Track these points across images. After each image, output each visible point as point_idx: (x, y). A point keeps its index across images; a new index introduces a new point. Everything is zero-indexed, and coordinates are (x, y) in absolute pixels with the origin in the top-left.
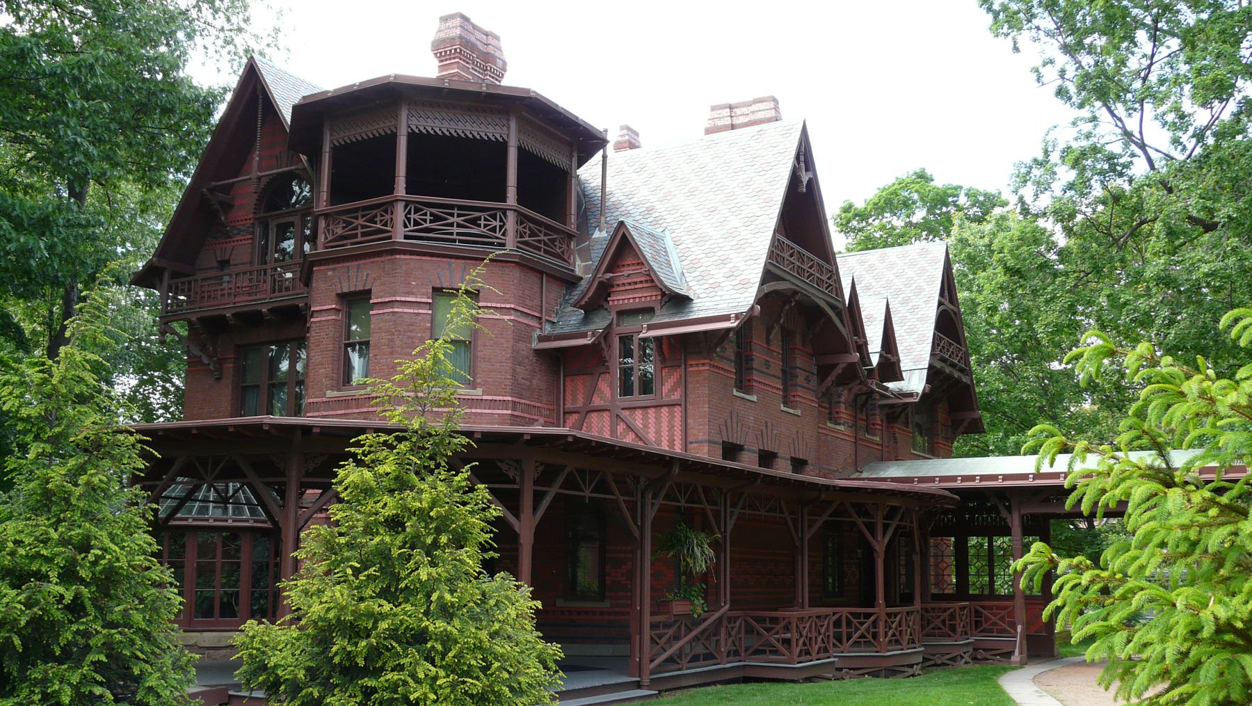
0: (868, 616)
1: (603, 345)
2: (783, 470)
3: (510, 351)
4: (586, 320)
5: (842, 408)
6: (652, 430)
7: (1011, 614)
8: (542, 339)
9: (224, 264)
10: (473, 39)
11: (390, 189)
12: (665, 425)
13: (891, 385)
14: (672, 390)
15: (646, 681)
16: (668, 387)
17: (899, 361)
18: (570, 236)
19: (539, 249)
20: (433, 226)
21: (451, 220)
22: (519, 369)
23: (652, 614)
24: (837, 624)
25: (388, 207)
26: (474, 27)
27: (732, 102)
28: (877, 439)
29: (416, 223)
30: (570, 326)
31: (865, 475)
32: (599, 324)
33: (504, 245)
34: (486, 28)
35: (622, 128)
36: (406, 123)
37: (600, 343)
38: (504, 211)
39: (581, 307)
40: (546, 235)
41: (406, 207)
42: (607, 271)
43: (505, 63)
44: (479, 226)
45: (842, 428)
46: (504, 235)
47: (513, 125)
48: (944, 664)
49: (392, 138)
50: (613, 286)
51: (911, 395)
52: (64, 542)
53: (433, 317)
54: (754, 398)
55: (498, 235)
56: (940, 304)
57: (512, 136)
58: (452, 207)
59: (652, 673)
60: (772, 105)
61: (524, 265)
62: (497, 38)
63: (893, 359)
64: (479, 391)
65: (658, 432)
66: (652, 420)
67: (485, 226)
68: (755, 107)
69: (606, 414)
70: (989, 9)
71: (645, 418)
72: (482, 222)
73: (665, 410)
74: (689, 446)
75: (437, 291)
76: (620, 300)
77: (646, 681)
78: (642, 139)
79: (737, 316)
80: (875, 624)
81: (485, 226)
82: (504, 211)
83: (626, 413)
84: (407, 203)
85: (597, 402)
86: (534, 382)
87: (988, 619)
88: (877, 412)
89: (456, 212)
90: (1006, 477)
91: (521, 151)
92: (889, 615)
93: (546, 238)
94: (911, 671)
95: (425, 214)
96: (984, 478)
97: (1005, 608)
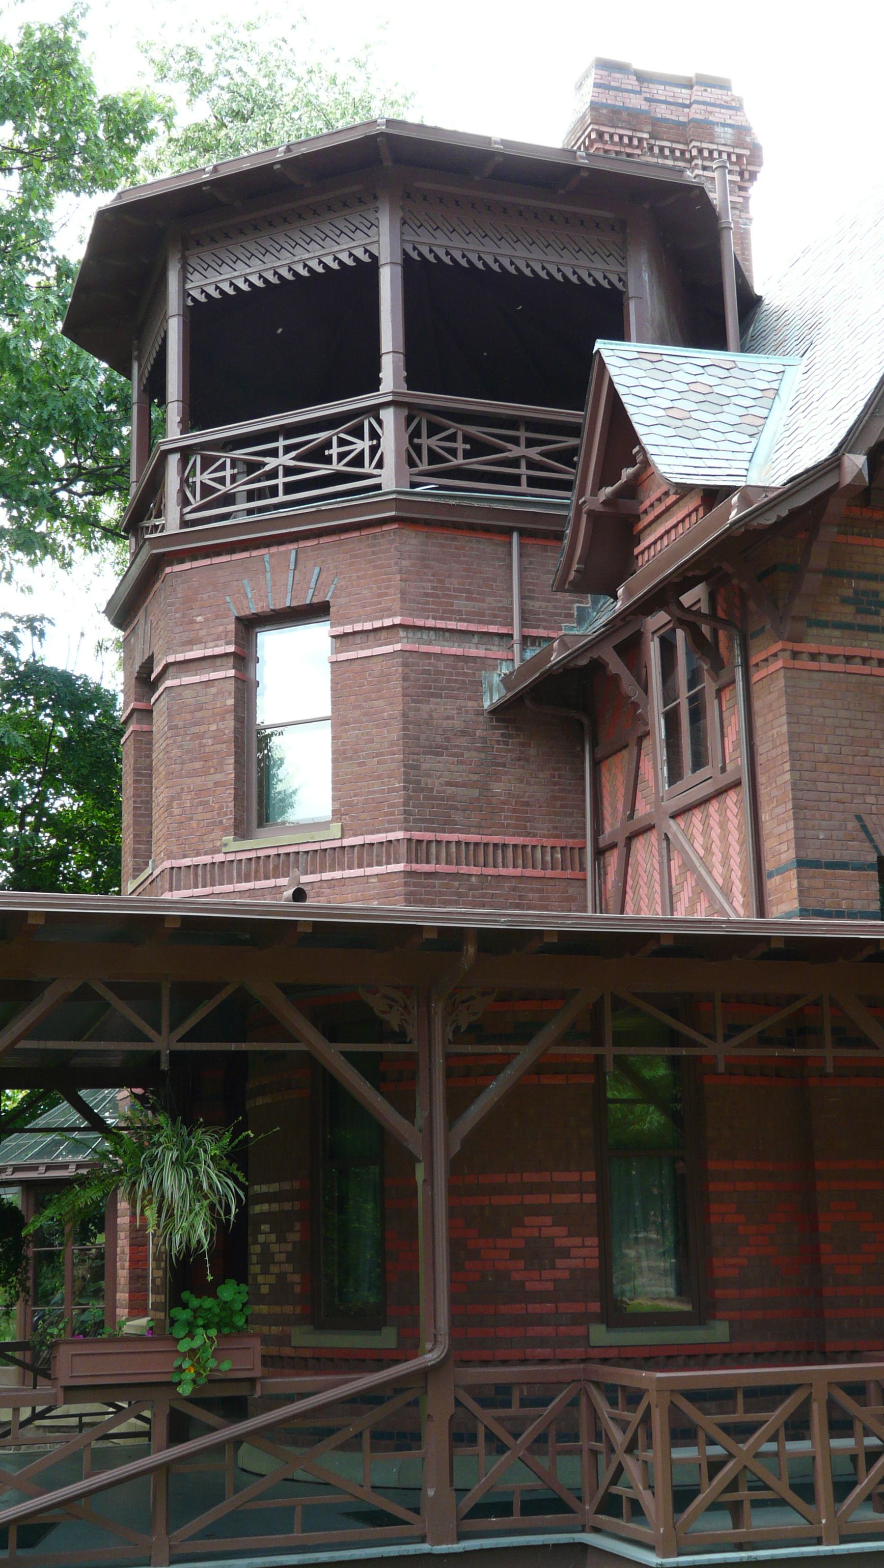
1: (615, 665)
3: (397, 725)
6: (717, 859)
10: (636, 102)
19: (515, 480)
21: (271, 463)
22: (428, 763)
26: (642, 77)
29: (207, 490)
33: (378, 487)
34: (688, 71)
37: (598, 665)
38: (374, 411)
40: (530, 443)
41: (184, 461)
43: (742, 131)
44: (328, 460)
46: (380, 465)
50: (638, 518)
53: (245, 690)
55: (367, 469)
61: (409, 517)
62: (723, 85)
65: (726, 861)
67: (341, 456)
69: (653, 837)
71: (706, 833)
72: (334, 451)
74: (771, 884)
81: (341, 456)
82: (374, 411)
83: (674, 827)
85: (643, 809)
86: (497, 788)
89: (281, 443)
93: (533, 453)
95: (222, 467)
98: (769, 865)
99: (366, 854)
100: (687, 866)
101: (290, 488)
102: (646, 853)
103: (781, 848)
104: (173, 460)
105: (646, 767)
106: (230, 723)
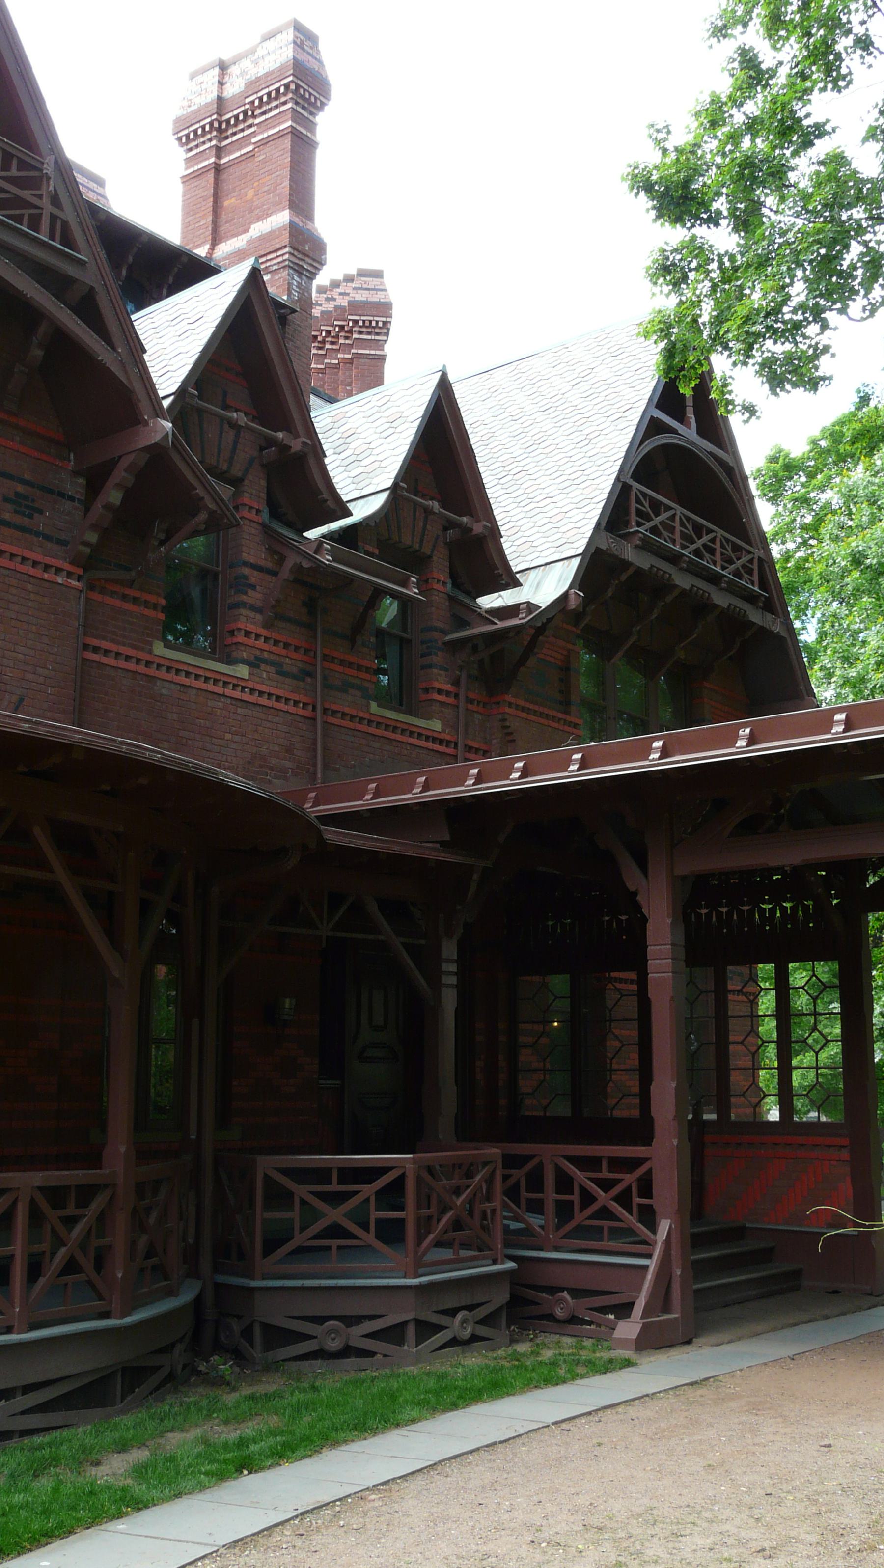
5: (248, 621)
7: (646, 1187)
17: (495, 533)
28: (436, 725)
45: (243, 671)
48: (347, 1352)
56: (651, 428)
60: (289, 35)
63: (478, 528)
87: (587, 1198)
88: (438, 658)
97: (633, 1164)
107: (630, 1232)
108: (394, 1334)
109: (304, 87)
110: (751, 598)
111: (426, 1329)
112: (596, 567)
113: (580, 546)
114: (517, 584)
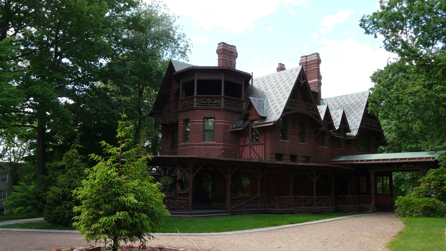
0: (311, 198)
2: (286, 161)
4: (244, 123)
6: (258, 151)
7: (371, 199)
8: (232, 128)
9: (169, 110)
10: (227, 48)
11: (193, 94)
12: (261, 149)
13: (348, 134)
14: (262, 140)
15: (229, 212)
16: (262, 141)
18: (242, 101)
20: (204, 102)
23: (231, 196)
24: (301, 200)
25: (193, 98)
26: (227, 45)
27: (306, 55)
29: (199, 102)
30: (240, 125)
31: (335, 160)
32: (246, 124)
35: (279, 64)
36: (196, 78)
38: (221, 97)
39: (242, 120)
42: (247, 111)
43: (237, 53)
45: (326, 147)
47: (223, 75)
49: (193, 81)
51: (352, 137)
52: (69, 182)
53: (204, 125)
54: (288, 141)
57: (223, 78)
58: (208, 97)
59: (230, 210)
61: (225, 110)
62: (235, 47)
63: (347, 127)
64: (215, 142)
65: (259, 151)
66: (258, 148)
68: (312, 56)
70: (364, 28)
71: (257, 148)
73: (261, 146)
75: (204, 118)
76: (251, 118)
77: (229, 212)
78: (286, 67)
79: (273, 122)
80: (313, 200)
82: (221, 97)
84: (197, 97)
85: (246, 143)
87: (365, 200)
90: (375, 160)
91: (225, 82)
92: (318, 198)
94: (326, 213)
96: (361, 161)
98: (266, 153)
99: (218, 145)
100: (253, 150)
101: (210, 104)
102: (247, 149)
103: (268, 151)
104: (195, 98)
105: (248, 139)
106: (202, 129)
107: (370, 203)
108: (350, 211)
109: (318, 61)
110: (377, 128)
111: (353, 210)
112: (360, 129)
113: (358, 127)
114: (351, 132)
